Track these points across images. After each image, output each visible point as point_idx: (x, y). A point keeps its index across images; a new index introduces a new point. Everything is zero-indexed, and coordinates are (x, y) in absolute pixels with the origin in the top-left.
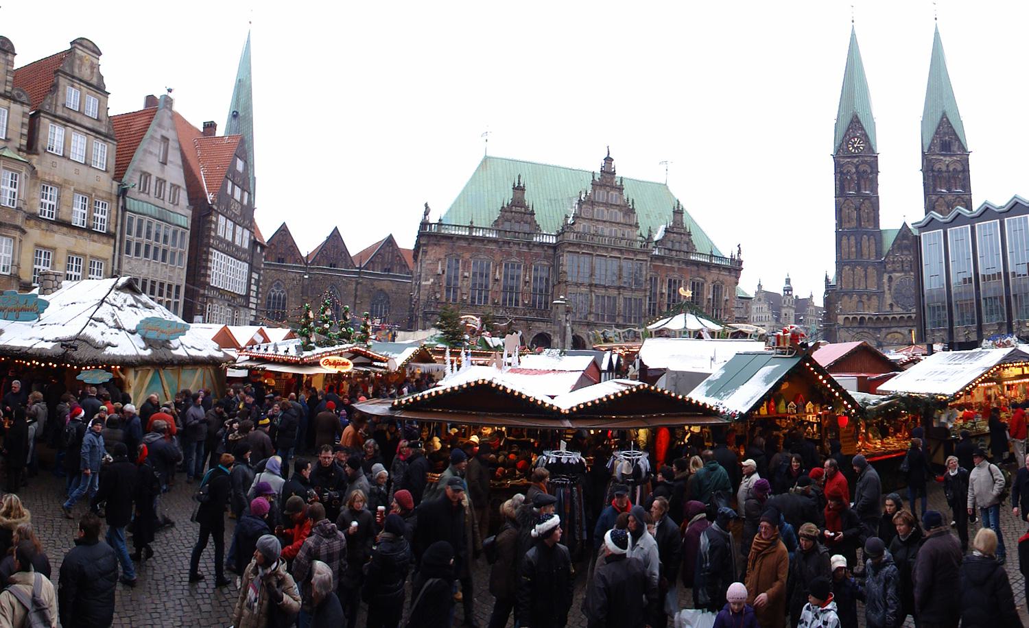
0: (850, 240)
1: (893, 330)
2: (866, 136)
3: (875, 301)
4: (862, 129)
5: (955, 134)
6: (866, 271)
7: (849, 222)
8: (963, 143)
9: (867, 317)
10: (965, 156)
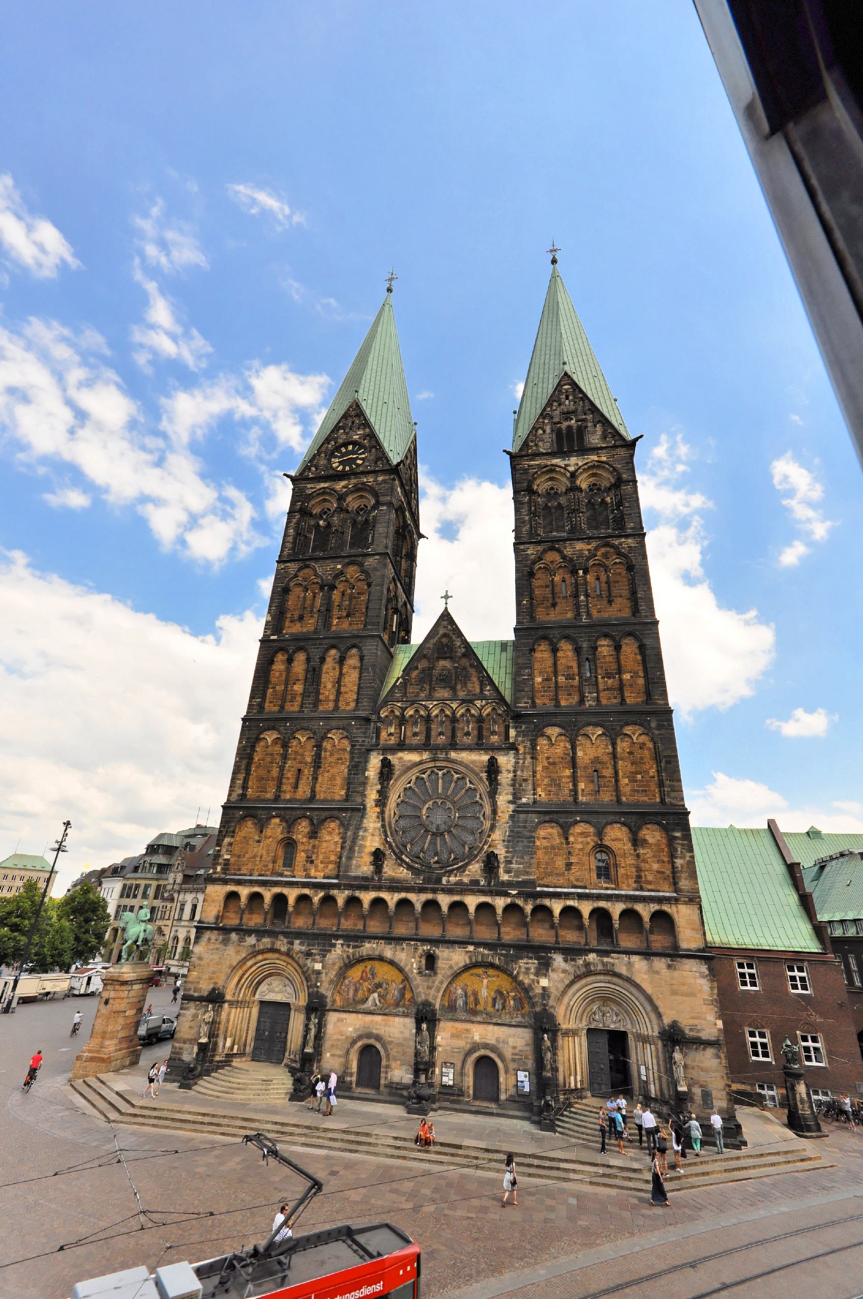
0: (295, 664)
1: (368, 948)
2: (372, 436)
3: (331, 837)
4: (366, 424)
5: (594, 409)
6: (319, 747)
7: (301, 618)
8: (616, 425)
9: (292, 895)
10: (622, 452)
